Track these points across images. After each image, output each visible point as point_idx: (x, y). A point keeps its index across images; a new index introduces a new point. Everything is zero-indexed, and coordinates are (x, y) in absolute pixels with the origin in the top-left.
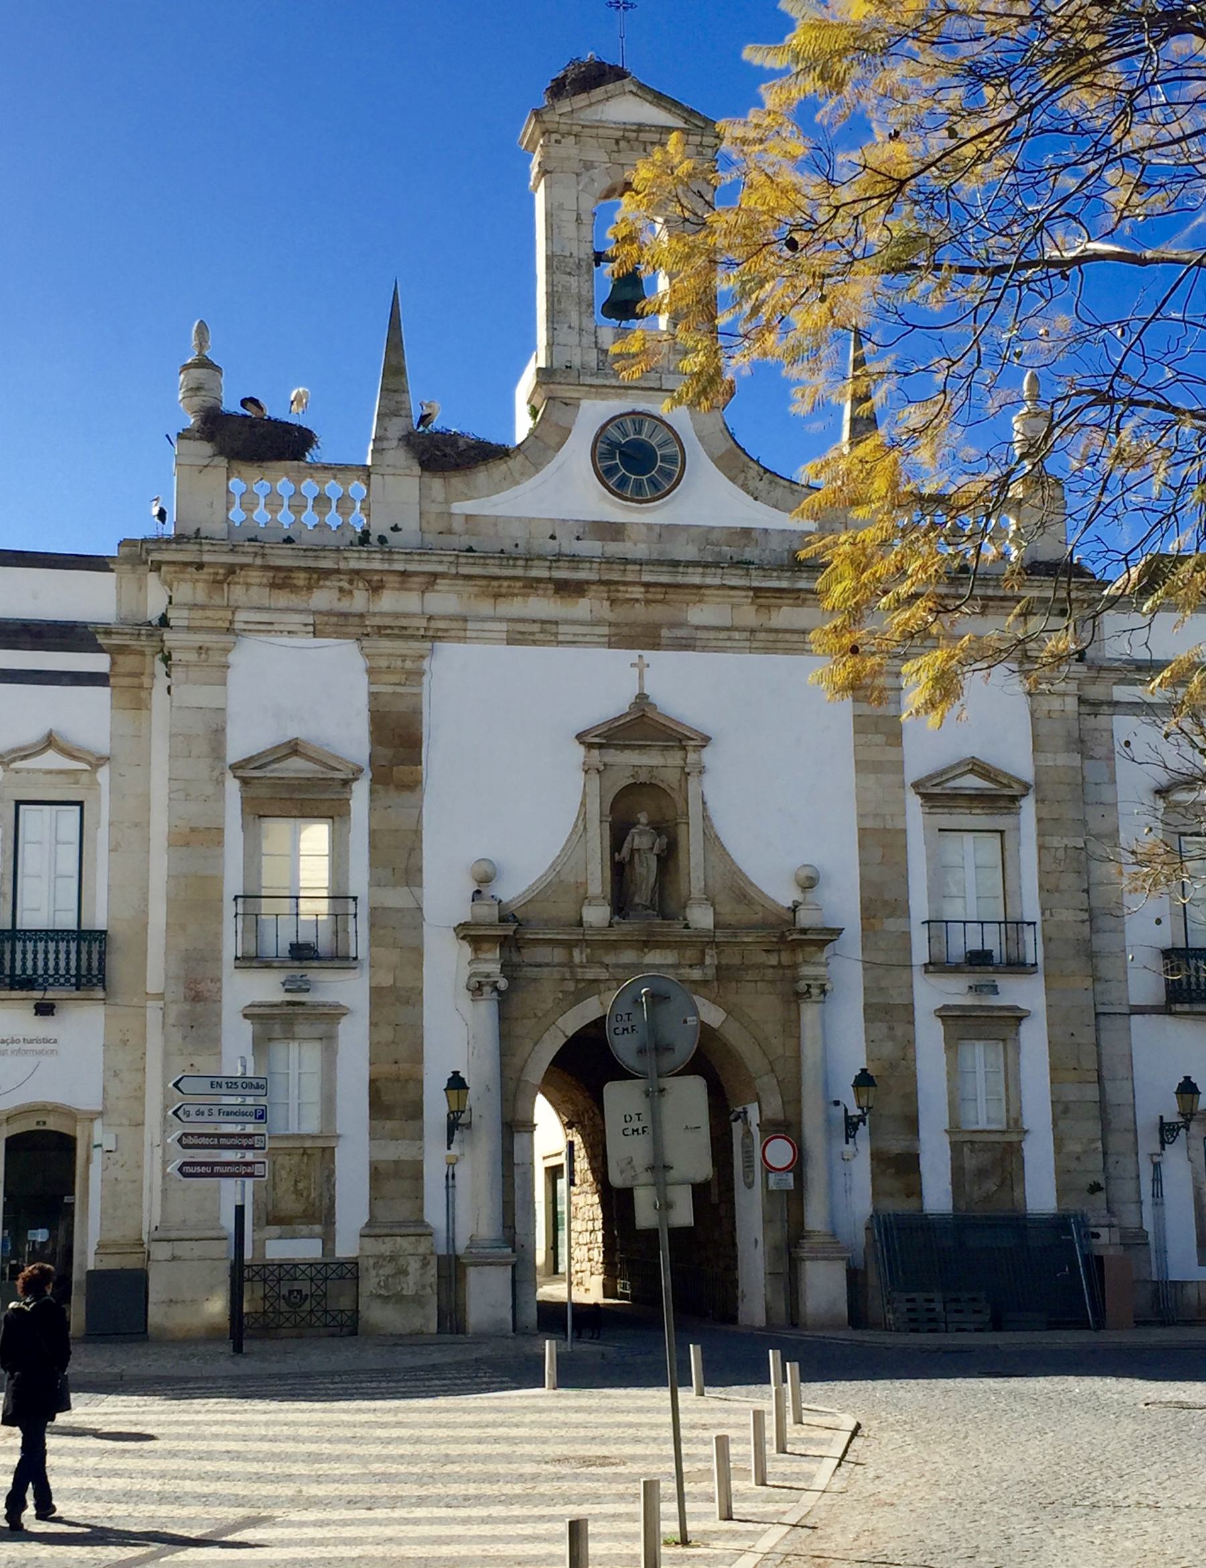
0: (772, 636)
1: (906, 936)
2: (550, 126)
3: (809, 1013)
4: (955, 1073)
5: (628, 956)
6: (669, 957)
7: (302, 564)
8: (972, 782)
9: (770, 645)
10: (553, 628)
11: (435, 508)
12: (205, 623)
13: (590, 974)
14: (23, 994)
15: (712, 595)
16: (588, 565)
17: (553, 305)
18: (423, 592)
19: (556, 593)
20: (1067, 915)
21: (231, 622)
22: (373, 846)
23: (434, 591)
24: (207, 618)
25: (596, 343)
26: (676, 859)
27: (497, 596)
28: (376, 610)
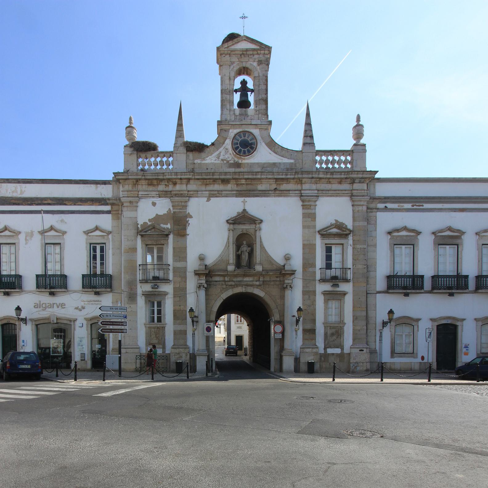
0: (280, 192)
1: (315, 273)
2: (222, 52)
3: (288, 293)
4: (326, 308)
5: (239, 279)
6: (251, 279)
7: (154, 177)
8: (335, 230)
9: (280, 195)
10: (221, 192)
11: (191, 162)
12: (131, 195)
13: (230, 283)
14: (91, 290)
15: (264, 181)
16: (229, 174)
17: (222, 103)
18: (187, 185)
19: (222, 183)
20: (360, 266)
21: (138, 195)
22: (174, 252)
23: (189, 184)
24: (132, 194)
25: (234, 114)
26: (253, 253)
27: (206, 185)
28: (175, 189)
